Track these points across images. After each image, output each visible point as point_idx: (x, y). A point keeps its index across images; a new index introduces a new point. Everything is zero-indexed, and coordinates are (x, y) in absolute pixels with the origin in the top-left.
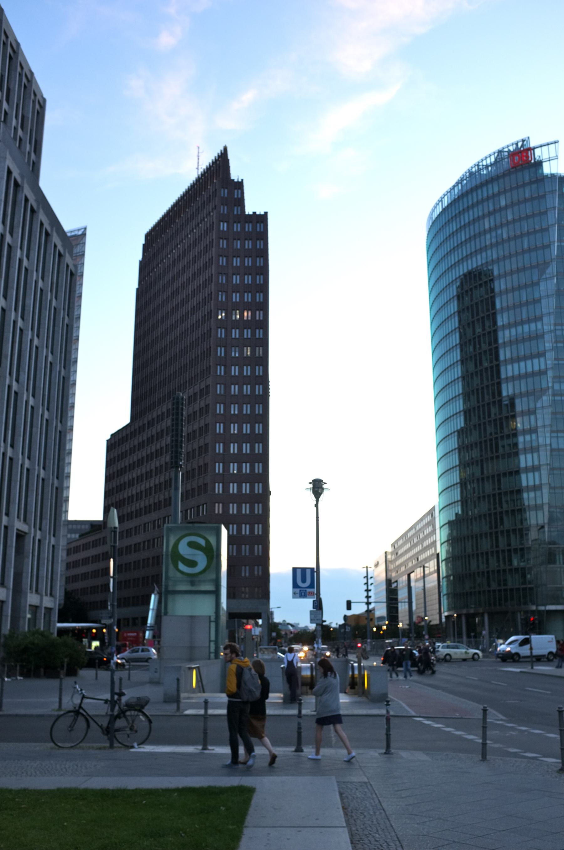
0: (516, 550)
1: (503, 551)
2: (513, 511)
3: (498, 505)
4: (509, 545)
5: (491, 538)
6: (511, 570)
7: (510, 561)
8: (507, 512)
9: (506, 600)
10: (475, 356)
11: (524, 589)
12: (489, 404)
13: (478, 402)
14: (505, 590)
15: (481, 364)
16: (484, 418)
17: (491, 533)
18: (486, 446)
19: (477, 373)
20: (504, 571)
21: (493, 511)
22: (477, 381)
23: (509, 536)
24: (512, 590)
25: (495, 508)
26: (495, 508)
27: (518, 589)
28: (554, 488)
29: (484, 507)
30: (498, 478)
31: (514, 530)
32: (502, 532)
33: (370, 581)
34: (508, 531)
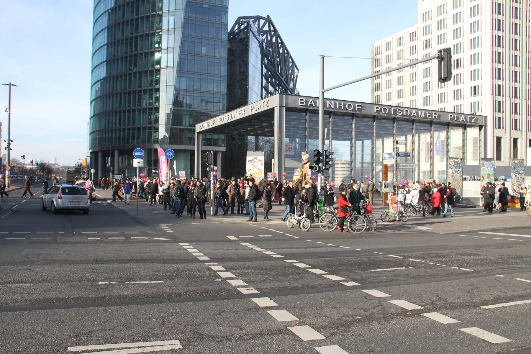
0: (145, 91)
3: (133, 49)
4: (140, 86)
6: (139, 110)
7: (140, 102)
8: (141, 54)
17: (126, 75)
20: (134, 110)
23: (140, 78)
24: (139, 129)
25: (131, 52)
26: (131, 52)
27: (144, 128)
29: (121, 50)
32: (135, 73)
34: (140, 73)
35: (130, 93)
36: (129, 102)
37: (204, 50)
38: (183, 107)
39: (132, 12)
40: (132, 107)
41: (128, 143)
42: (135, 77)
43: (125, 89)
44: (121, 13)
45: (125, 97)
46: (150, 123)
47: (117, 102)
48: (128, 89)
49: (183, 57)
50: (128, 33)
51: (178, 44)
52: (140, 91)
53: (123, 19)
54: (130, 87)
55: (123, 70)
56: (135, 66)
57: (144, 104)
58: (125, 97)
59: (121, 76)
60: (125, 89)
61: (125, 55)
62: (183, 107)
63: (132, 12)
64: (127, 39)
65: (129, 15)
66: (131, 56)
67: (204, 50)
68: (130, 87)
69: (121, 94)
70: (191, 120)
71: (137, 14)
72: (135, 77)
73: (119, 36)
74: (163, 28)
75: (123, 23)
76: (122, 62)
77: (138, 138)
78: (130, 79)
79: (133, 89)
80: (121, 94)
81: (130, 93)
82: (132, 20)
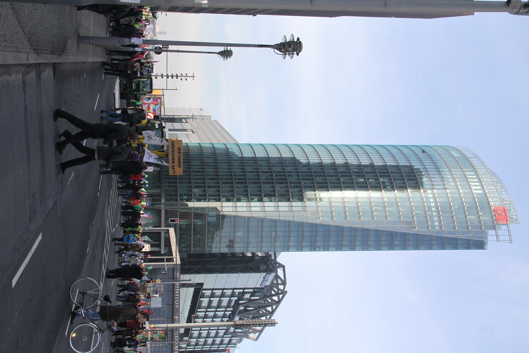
0: (205, 191)
1: (204, 183)
2: (233, 191)
3: (237, 181)
4: (209, 187)
5: (214, 175)
6: (190, 187)
7: (197, 187)
8: (232, 187)
9: (169, 183)
10: (350, 172)
11: (176, 195)
12: (312, 179)
13: (314, 172)
14: (176, 183)
15: (342, 176)
16: (302, 176)
17: (217, 175)
18: (282, 176)
19: (337, 173)
20: (190, 183)
21: (234, 178)
22: (331, 172)
23: (215, 187)
24: (176, 187)
25: (235, 179)
26: (235, 179)
27: (176, 191)
28: (248, 222)
29: (237, 171)
30: (257, 182)
31: (219, 191)
32: (218, 183)
33: (183, 78)
34: (219, 187)
35: (204, 179)
36: (197, 179)
37: (239, 234)
38: (194, 219)
39: (267, 179)
40: (193, 181)
41: (166, 179)
42: (215, 183)
43: (207, 175)
44: (266, 170)
45: (200, 175)
46: (181, 195)
47: (197, 169)
48: (206, 177)
49: (233, 218)
50: (249, 176)
51: (239, 214)
52: (204, 187)
53: (261, 172)
54: (208, 179)
55: (221, 174)
56: (224, 183)
57: (195, 190)
58: (200, 175)
59: (217, 172)
60: (207, 175)
61: (233, 174)
62: (194, 219)
63: (267, 179)
64: (245, 175)
65: (263, 176)
66: (232, 179)
67: (239, 234)
68: (208, 179)
69: (203, 172)
70: (184, 226)
71: (264, 183)
72: (215, 183)
73: (248, 169)
74: (279, 203)
75: (258, 172)
76: (228, 172)
77: (169, 187)
78: (214, 179)
79: (207, 181)
80: (203, 172)
81: (204, 179)
82: (259, 179)
